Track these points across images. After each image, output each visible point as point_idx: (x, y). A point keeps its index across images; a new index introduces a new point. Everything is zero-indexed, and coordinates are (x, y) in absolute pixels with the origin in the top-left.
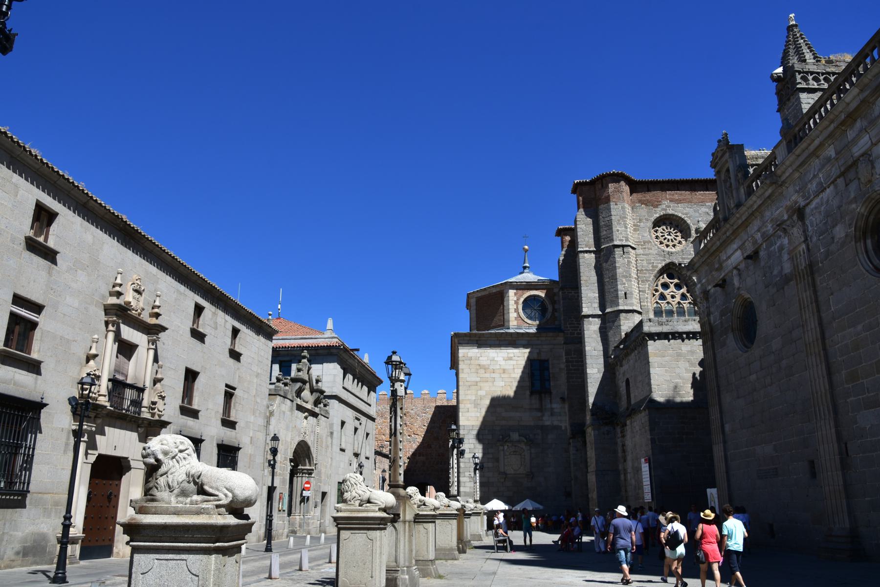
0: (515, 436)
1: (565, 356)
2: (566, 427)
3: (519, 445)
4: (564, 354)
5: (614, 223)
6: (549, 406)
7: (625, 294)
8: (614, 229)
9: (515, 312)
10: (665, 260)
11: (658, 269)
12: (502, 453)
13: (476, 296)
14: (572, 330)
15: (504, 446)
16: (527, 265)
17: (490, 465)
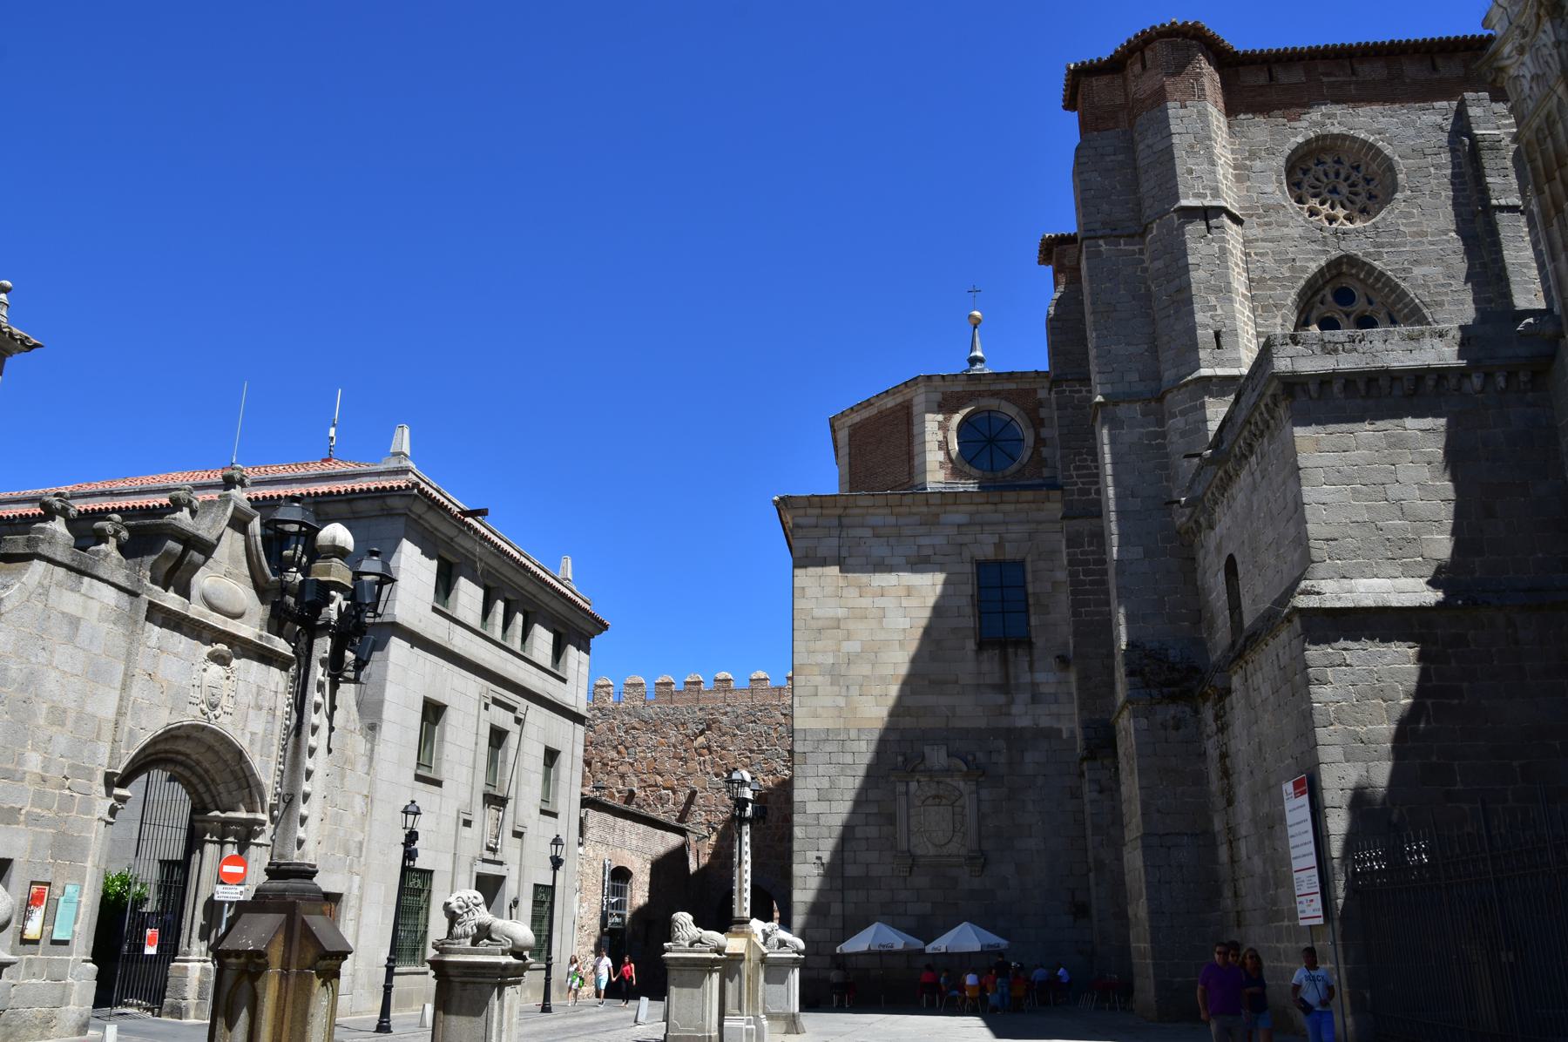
0: (937, 757)
1: (1068, 547)
2: (1072, 732)
3: (948, 780)
4: (1064, 547)
5: (1179, 153)
6: (1026, 678)
7: (1217, 335)
8: (1180, 169)
9: (940, 448)
10: (1326, 252)
11: (1306, 276)
12: (902, 801)
13: (849, 423)
14: (1083, 483)
15: (907, 783)
16: (979, 353)
17: (873, 831)
